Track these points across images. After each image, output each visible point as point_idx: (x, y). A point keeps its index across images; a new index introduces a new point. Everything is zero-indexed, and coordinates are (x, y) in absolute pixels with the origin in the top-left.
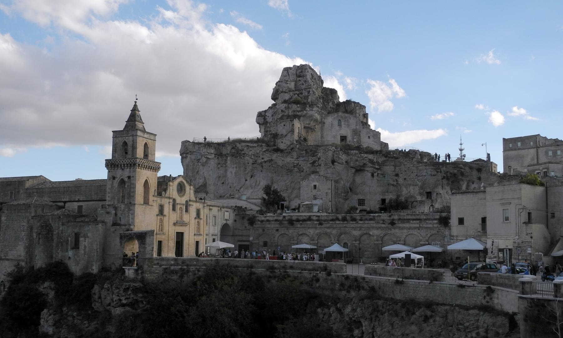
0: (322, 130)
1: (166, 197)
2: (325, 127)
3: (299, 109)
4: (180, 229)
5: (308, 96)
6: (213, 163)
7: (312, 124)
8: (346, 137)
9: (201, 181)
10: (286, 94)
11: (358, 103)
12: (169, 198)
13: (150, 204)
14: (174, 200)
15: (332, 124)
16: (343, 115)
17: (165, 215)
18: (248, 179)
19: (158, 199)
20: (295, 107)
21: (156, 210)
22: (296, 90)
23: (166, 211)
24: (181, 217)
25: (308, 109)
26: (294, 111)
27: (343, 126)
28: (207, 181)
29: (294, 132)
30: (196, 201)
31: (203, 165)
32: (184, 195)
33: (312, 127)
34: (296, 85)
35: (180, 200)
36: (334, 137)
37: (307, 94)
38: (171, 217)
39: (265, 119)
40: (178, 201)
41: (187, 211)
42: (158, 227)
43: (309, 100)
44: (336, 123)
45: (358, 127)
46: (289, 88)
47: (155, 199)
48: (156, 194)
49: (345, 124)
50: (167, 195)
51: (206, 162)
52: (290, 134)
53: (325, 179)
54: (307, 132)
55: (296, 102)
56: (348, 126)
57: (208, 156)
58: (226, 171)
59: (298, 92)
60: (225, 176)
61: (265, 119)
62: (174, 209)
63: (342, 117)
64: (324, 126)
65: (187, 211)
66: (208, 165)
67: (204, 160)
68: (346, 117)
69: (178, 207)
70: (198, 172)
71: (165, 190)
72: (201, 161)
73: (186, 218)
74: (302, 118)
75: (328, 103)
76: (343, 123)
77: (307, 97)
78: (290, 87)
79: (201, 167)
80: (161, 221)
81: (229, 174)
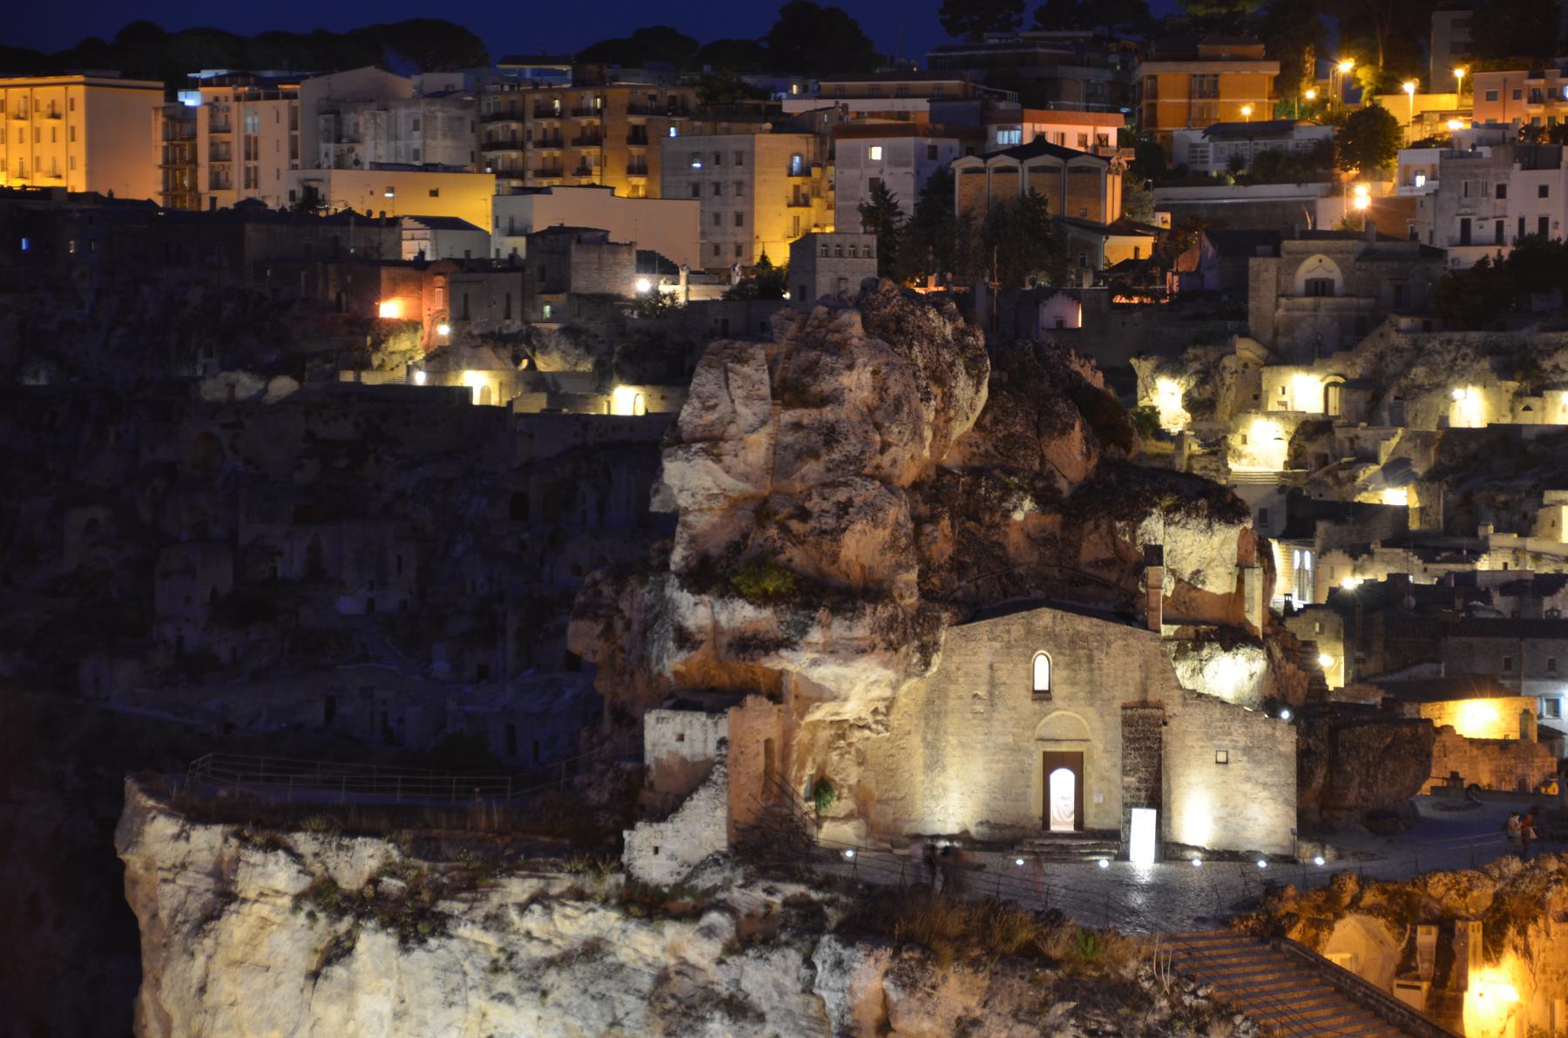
15: (992, 684)
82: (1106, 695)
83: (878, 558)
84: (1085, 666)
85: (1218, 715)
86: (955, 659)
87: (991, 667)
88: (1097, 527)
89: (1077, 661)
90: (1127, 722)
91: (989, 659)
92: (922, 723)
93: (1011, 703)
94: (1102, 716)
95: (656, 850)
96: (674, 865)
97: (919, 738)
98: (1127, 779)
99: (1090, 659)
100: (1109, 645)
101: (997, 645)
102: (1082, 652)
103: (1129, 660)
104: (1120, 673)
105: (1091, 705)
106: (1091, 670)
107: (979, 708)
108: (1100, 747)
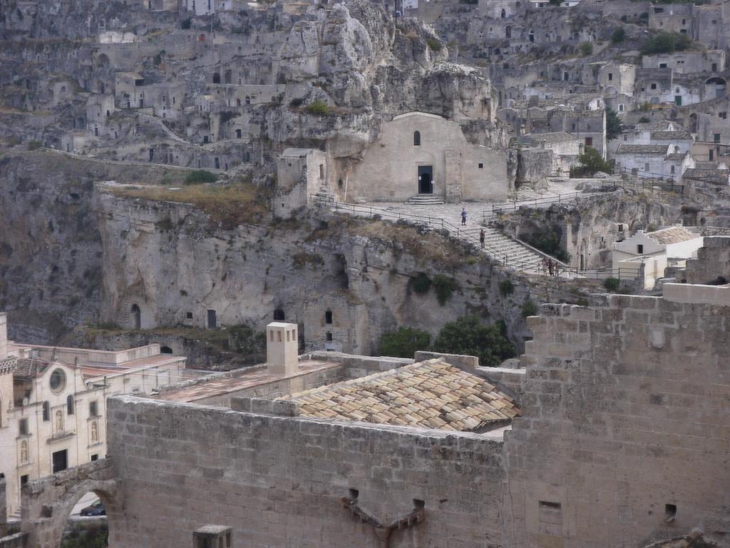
1: (32, 405)
3: (320, 127)
4: (58, 447)
5: (343, 90)
6: (154, 241)
7: (353, 151)
8: (431, 167)
9: (131, 279)
10: (299, 86)
12: (37, 404)
13: (3, 425)
14: (46, 405)
17: (31, 435)
18: (219, 281)
19: (19, 415)
20: (312, 121)
21: (14, 429)
22: (320, 75)
23: (32, 428)
24: (61, 427)
25: (339, 124)
26: (311, 131)
28: (144, 277)
29: (305, 183)
30: (88, 391)
31: (134, 246)
32: (63, 389)
33: (355, 156)
34: (320, 63)
35: (58, 400)
37: (340, 85)
38: (41, 429)
39: (264, 128)
40: (52, 404)
41: (70, 411)
42: (20, 455)
43: (347, 99)
46: (303, 73)
47: (11, 415)
48: (12, 408)
50: (31, 402)
51: (139, 239)
52: (298, 187)
53: (346, 305)
54: (344, 166)
55: (316, 111)
57: (142, 228)
58: (176, 261)
59: (323, 80)
60: (175, 272)
61: (264, 128)
62: (46, 417)
65: (70, 411)
66: (144, 245)
67: (137, 235)
69: (53, 414)
70: (124, 257)
71: (28, 394)
72: (129, 236)
73: (69, 423)
74: (328, 145)
75: (403, 81)
77: (340, 93)
78: (306, 70)
79: (130, 250)
80: (25, 444)
81: (182, 269)
88: (435, 85)
95: (283, 205)
96: (290, 211)
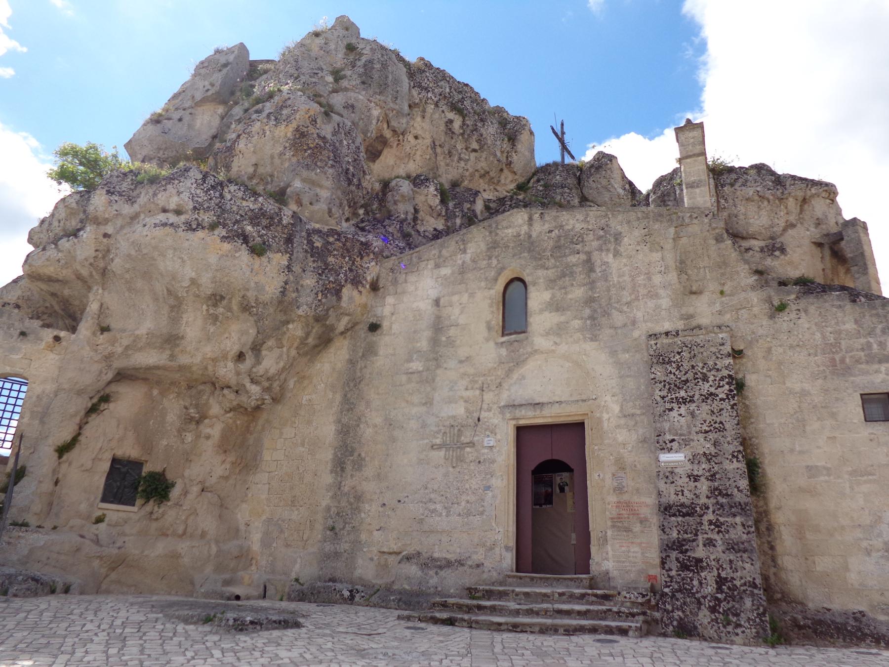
0: (352, 384)
2: (381, 361)
8: (578, 427)
11: (761, 169)
15: (438, 327)
16: (538, 228)
27: (540, 320)
36: (456, 442)
44: (477, 309)
45: (705, 310)
49: (556, 306)
56: (596, 315)
63: (528, 246)
64: (370, 351)
68: (566, 243)
76: (537, 298)
82: (618, 319)
83: (277, 161)
84: (581, 278)
85: (850, 326)
86: (390, 300)
87: (437, 302)
89: (566, 273)
90: (661, 359)
91: (433, 294)
92: (339, 397)
93: (463, 352)
94: (613, 353)
97: (331, 419)
98: (665, 457)
99: (589, 265)
100: (618, 237)
101: (446, 271)
102: (573, 259)
103: (656, 256)
104: (641, 279)
105: (594, 338)
106: (592, 284)
107: (417, 365)
108: (616, 408)
